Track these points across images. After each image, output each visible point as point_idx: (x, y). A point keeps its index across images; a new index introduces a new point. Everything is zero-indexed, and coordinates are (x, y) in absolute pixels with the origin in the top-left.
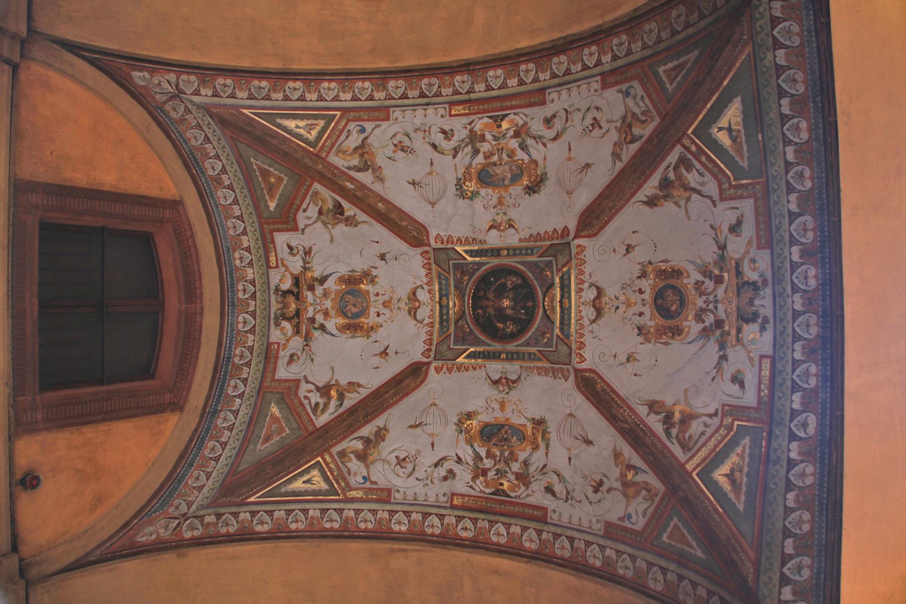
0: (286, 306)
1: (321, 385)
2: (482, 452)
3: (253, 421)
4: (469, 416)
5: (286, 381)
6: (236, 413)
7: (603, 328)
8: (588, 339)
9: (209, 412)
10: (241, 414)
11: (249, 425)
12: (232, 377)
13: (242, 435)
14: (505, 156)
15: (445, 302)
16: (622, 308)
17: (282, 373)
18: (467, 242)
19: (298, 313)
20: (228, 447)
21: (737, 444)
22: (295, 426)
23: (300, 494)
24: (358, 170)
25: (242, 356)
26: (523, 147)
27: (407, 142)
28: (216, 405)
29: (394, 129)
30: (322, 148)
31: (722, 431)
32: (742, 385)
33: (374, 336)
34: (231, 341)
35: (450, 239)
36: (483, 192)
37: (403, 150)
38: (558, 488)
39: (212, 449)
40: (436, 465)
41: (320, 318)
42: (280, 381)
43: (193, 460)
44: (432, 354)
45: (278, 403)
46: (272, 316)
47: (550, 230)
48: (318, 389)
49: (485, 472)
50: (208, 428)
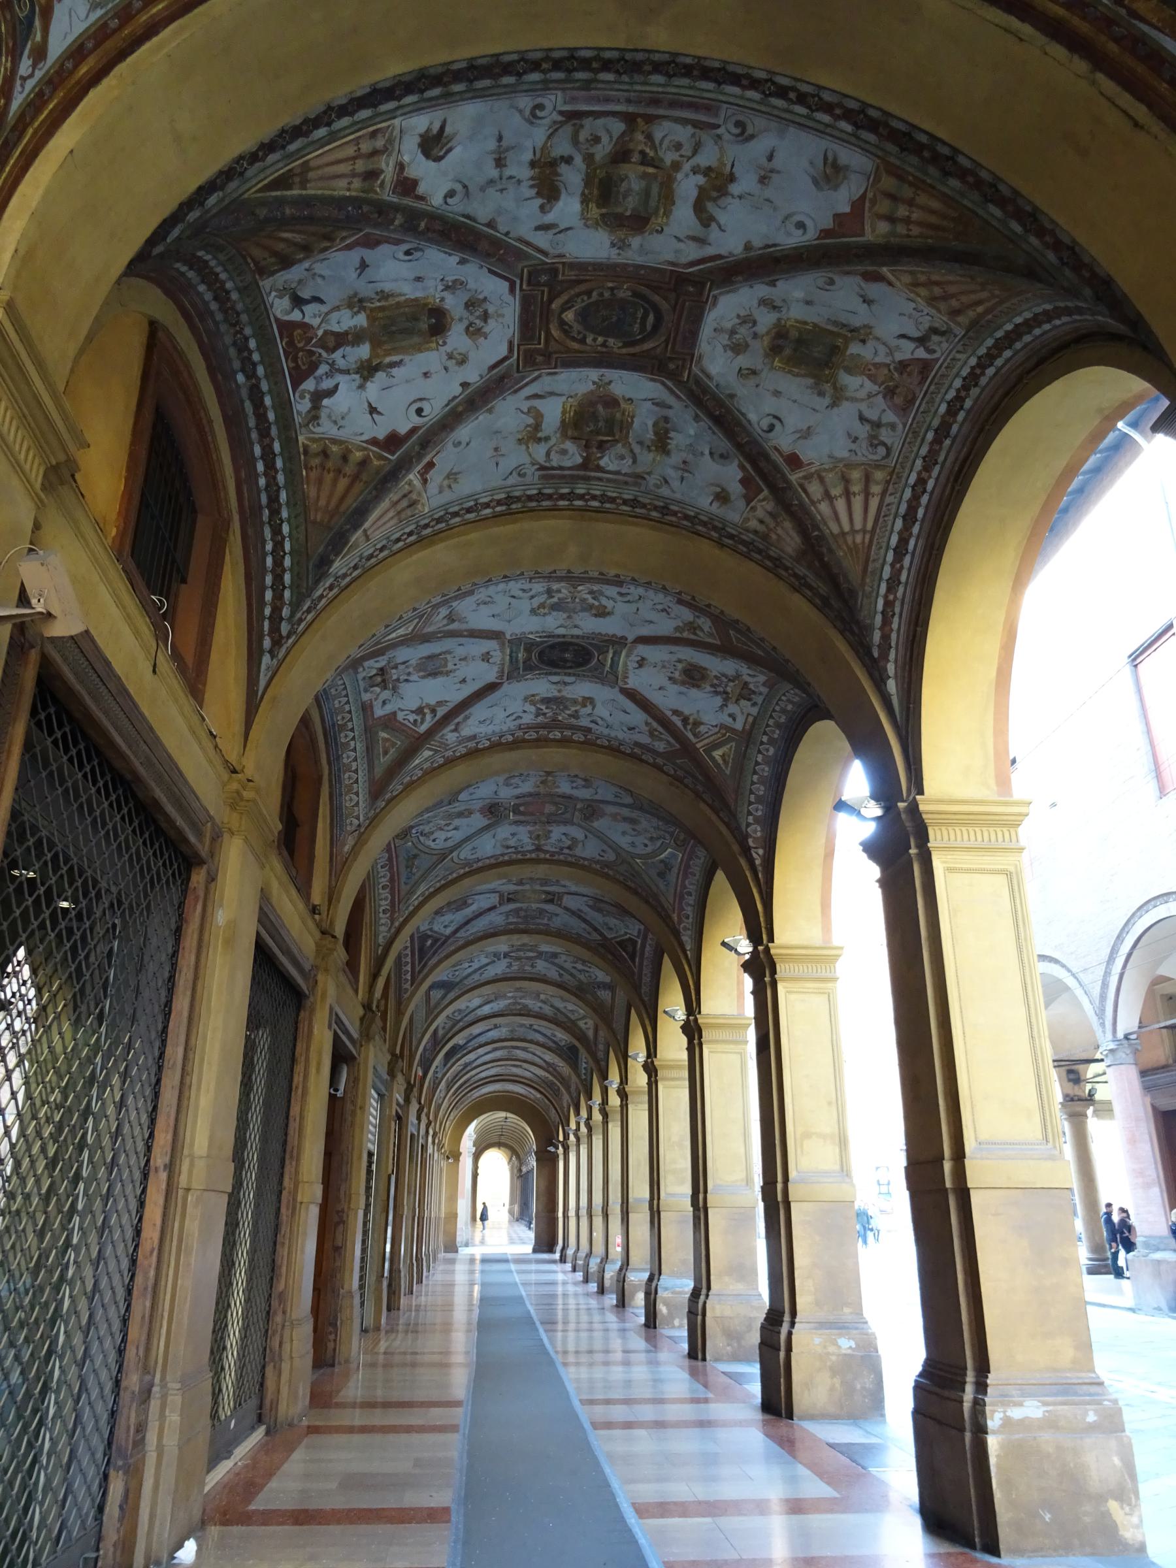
2: (543, 707)
3: (370, 750)
6: (354, 750)
7: (643, 672)
8: (631, 675)
12: (340, 732)
17: (379, 712)
19: (384, 681)
26: (594, 598)
32: (734, 719)
33: (452, 675)
36: (555, 613)
38: (600, 722)
39: (349, 778)
41: (402, 678)
42: (380, 718)
47: (611, 633)
48: (412, 712)
49: (544, 714)
50: (339, 769)
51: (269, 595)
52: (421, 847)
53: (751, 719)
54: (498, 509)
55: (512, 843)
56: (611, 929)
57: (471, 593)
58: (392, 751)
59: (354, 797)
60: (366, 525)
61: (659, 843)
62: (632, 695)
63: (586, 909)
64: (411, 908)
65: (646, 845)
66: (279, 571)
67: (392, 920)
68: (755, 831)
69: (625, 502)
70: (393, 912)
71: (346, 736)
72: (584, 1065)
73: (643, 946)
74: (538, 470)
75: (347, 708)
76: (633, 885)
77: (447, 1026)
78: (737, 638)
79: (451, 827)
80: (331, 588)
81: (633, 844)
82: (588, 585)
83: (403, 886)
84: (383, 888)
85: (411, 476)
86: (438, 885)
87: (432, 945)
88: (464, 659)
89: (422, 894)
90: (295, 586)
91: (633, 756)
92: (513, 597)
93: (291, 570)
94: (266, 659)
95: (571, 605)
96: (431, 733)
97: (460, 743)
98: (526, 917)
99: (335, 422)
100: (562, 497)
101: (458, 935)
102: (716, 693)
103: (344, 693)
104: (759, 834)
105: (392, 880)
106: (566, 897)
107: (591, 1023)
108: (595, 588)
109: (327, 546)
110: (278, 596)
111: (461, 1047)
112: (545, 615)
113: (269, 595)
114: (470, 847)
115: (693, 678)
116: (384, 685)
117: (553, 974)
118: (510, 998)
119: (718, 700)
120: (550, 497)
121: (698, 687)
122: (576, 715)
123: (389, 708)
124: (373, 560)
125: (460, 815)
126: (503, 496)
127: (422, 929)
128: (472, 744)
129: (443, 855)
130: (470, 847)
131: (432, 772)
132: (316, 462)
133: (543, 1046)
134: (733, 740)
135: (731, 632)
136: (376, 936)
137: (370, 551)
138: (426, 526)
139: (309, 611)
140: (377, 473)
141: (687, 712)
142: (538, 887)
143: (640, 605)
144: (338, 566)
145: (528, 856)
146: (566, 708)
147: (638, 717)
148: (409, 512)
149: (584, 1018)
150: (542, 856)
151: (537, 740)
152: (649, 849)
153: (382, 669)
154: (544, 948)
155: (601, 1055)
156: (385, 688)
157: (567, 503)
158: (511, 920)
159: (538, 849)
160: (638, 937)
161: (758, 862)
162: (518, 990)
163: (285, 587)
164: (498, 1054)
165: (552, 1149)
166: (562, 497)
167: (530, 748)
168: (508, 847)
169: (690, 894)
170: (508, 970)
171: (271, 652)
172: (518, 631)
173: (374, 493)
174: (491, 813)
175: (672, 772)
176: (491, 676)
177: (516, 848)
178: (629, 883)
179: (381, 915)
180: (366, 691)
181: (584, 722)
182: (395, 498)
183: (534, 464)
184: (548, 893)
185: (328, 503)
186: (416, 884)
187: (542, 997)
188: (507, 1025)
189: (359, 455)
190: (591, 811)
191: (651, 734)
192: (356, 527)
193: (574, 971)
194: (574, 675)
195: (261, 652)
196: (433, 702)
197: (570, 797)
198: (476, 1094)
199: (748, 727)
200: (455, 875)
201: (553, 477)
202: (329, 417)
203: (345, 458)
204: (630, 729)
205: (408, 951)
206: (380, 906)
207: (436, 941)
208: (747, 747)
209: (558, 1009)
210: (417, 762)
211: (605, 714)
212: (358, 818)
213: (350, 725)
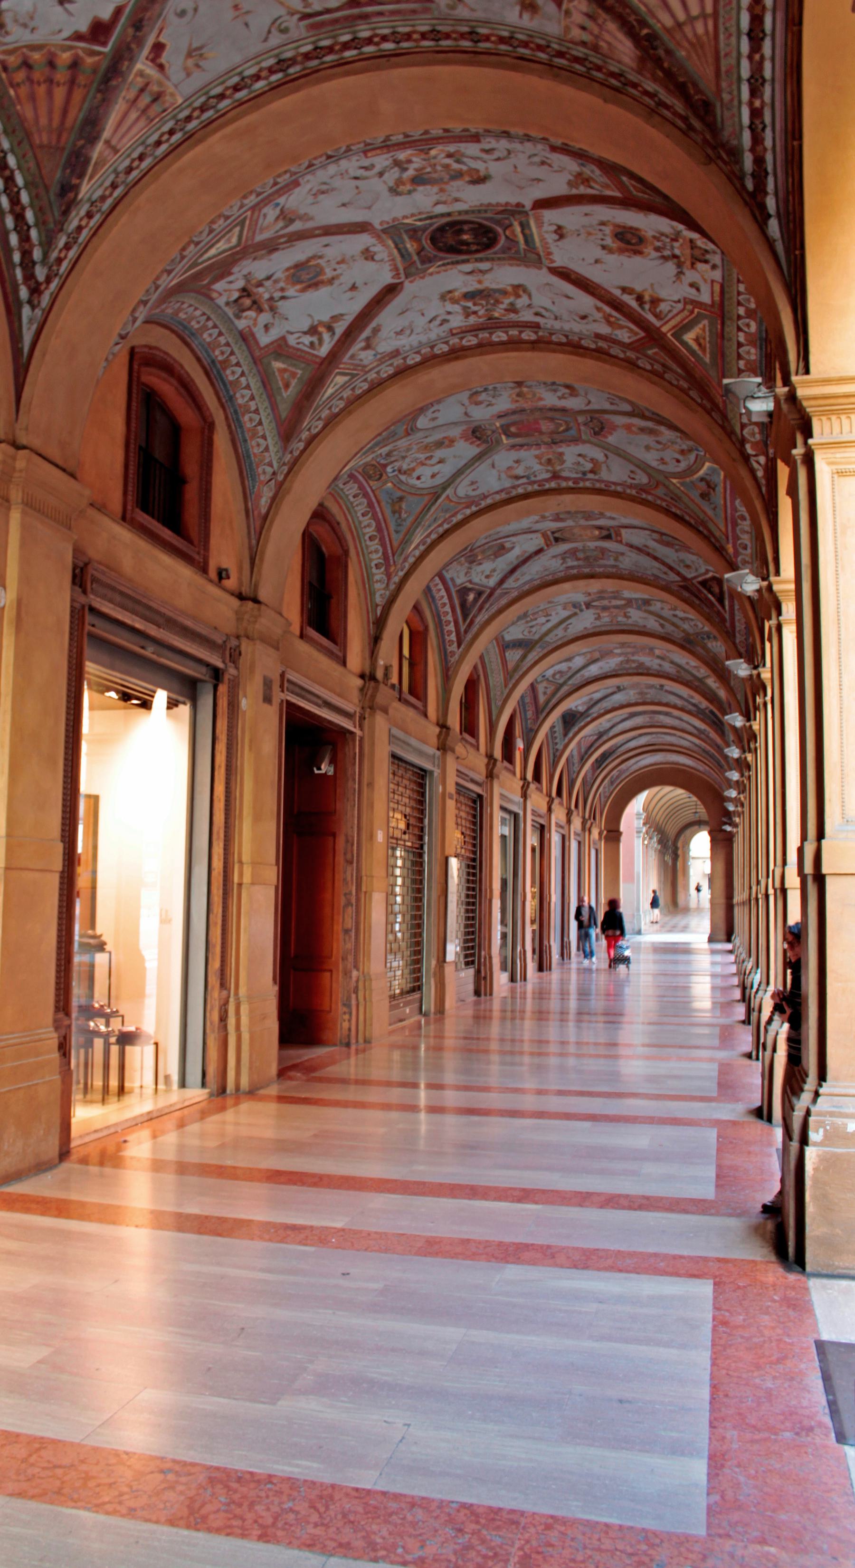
0: (242, 305)
1: (306, 329)
4: (450, 292)
5: (272, 343)
6: (248, 387)
8: (553, 249)
9: (226, 401)
10: (252, 385)
11: (265, 386)
12: (225, 369)
13: (264, 396)
14: (439, 168)
15: (401, 246)
16: (583, 236)
17: (264, 339)
18: (413, 215)
20: (261, 411)
21: (699, 322)
22: (303, 365)
23: (332, 394)
24: (286, 227)
25: (222, 353)
26: (458, 161)
27: (324, 187)
28: (227, 391)
29: (308, 187)
30: (247, 240)
31: (686, 313)
32: (698, 290)
33: (337, 282)
34: (207, 351)
35: (394, 220)
36: (421, 188)
37: (323, 192)
39: (251, 420)
40: (430, 321)
41: (277, 295)
42: (267, 346)
43: (243, 436)
44: (403, 276)
45: (276, 360)
46: (231, 316)
48: (305, 333)
49: (475, 313)
50: (236, 412)
51: (14, 239)
53: (717, 288)
54: (274, 78)
55: (520, 471)
56: (688, 567)
57: (296, 184)
58: (294, 382)
59: (261, 441)
60: (106, 135)
61: (692, 457)
62: (564, 274)
63: (652, 544)
64: (411, 560)
65: (678, 461)
66: (18, 209)
67: (389, 576)
68: (753, 434)
69: (424, 36)
71: (233, 373)
74: (301, 19)
75: (222, 340)
76: (678, 512)
77: (549, 691)
78: (634, 186)
80: (89, 215)
81: (662, 460)
82: (440, 147)
83: (394, 536)
85: (139, 66)
86: (441, 530)
87: (476, 600)
88: (342, 262)
89: (423, 542)
90: (40, 223)
91: (598, 350)
92: (356, 178)
93: (32, 205)
94: (26, 311)
95: (435, 176)
96: (334, 356)
97: (381, 361)
98: (586, 559)
99: (25, 26)
100: (346, 46)
101: (505, 586)
102: (665, 258)
103: (210, 324)
104: (758, 437)
105: (379, 529)
106: (623, 531)
108: (452, 148)
109: (64, 169)
110: (25, 238)
111: (583, 715)
112: (409, 192)
113: (14, 239)
114: (466, 482)
115: (628, 243)
116: (256, 306)
117: (652, 624)
118: (620, 655)
119: (670, 268)
120: (330, 50)
121: (640, 253)
122: (512, 309)
123: (275, 334)
124: (135, 174)
125: (439, 444)
126: (271, 62)
127: (458, 581)
128: (398, 362)
129: (435, 494)
131: (355, 402)
132: (20, 76)
133: (682, 709)
134: (705, 317)
135: (624, 179)
136: (372, 594)
137: (127, 163)
138: (189, 119)
139: (67, 247)
140: (95, 72)
141: (638, 288)
142: (582, 522)
143: (513, 160)
144: (86, 189)
145: (547, 486)
146: (498, 302)
147: (585, 302)
148: (156, 108)
149: (708, 677)
150: (564, 484)
151: (480, 345)
152: (683, 465)
153: (244, 290)
154: (627, 594)
156: (260, 310)
157: (354, 52)
158: (570, 563)
159: (555, 476)
161: (760, 474)
162: (623, 645)
163: (29, 227)
166: (346, 46)
167: (473, 356)
168: (517, 478)
169: (743, 518)
170: (598, 623)
171: (30, 302)
172: (387, 218)
173: (99, 96)
174: (479, 439)
175: (649, 367)
176: (386, 278)
177: (528, 477)
178: (674, 510)
179: (374, 570)
180: (238, 317)
181: (527, 316)
182: (132, 95)
183: (292, 14)
184: (600, 528)
185: (50, 120)
186: (410, 532)
187: (657, 652)
188: (633, 686)
189: (65, 57)
190: (598, 425)
191: (609, 323)
192: (93, 140)
193: (675, 620)
194: (487, 259)
195: (20, 305)
196: (326, 318)
197: (564, 410)
199: (717, 298)
200: (460, 517)
201: (322, 24)
202: (16, 21)
203: (51, 64)
204: (584, 317)
205: (448, 608)
206: (371, 560)
207: (479, 594)
208: (723, 324)
210: (330, 391)
211: (548, 304)
212: (270, 465)
213: (233, 360)
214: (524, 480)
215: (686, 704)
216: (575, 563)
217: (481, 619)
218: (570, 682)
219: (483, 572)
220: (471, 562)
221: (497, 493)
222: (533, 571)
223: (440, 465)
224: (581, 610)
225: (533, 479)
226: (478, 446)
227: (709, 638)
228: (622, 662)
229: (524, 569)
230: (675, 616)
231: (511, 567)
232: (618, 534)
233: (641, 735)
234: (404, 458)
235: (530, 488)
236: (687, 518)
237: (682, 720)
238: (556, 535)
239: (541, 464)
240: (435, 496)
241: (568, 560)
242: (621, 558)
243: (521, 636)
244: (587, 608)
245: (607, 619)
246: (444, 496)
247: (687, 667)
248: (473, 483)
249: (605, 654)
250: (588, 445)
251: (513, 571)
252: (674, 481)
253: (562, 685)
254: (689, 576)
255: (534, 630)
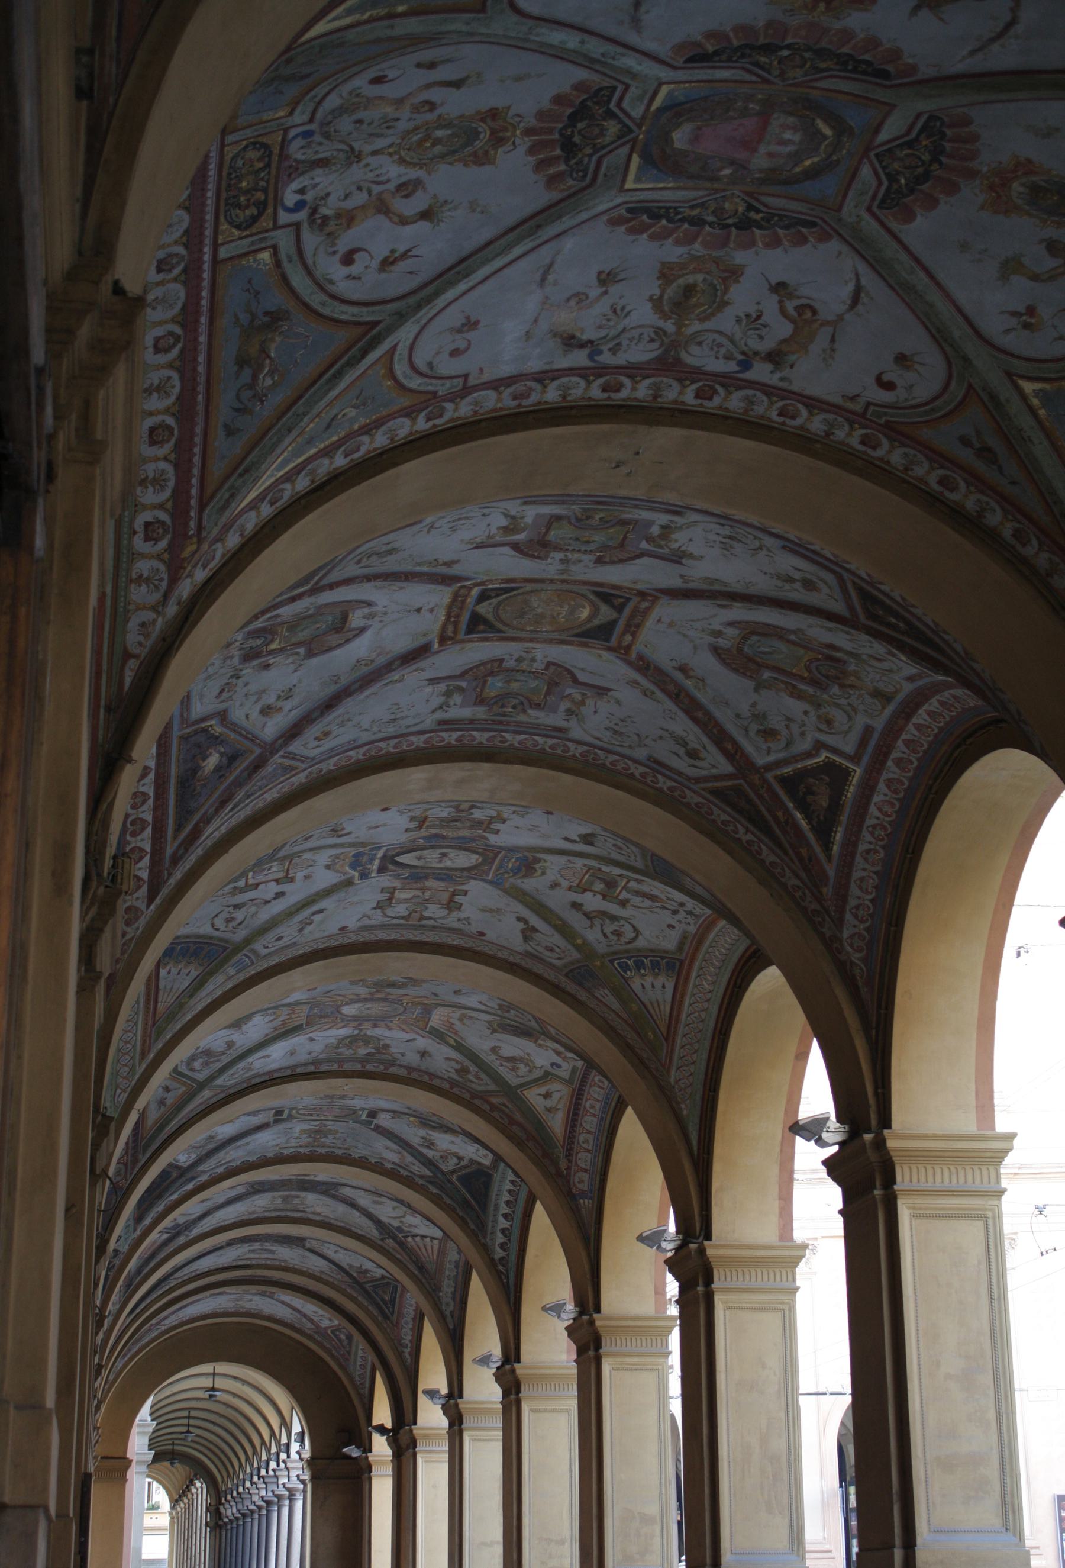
52: (298, 280)
55: (588, 323)
56: (769, 734)
64: (233, 540)
70: (180, 537)
72: (503, 1223)
73: (868, 788)
77: (171, 1099)
79: (419, 202)
84: (155, 436)
86: (325, 467)
98: (501, 699)
101: (296, 747)
105: (184, 409)
107: (560, 1092)
114: (453, 317)
118: (347, 1020)
127: (198, 709)
130: (453, 317)
133: (392, 1174)
150: (672, 392)
155: (582, 1181)
160: (855, 758)
164: (260, 1203)
165: (353, 1451)
168: (570, 342)
170: (378, 918)
174: (569, 148)
179: (138, 542)
184: (606, 595)
186: (261, 444)
187: (437, 1018)
193: (575, 920)
198: (173, 1317)
200: (381, 440)
206: (139, 507)
207: (233, 758)
209: (474, 1057)
214: (579, 358)
215: (409, 1159)
216: (467, 713)
217: (215, 830)
218: (219, 1082)
219: (261, 692)
220: (249, 656)
221: (496, 385)
222: (365, 720)
223: (423, 226)
224: (364, 875)
225: (606, 358)
226: (552, 181)
227: (639, 965)
228: (341, 1041)
229: (349, 705)
230: (576, 906)
231: (333, 688)
232: (633, 627)
233: (230, 1243)
234: (354, 156)
235: (578, 390)
236: (994, 518)
237: (353, 1205)
238: (484, 609)
239: (657, 303)
240: (368, 335)
241: (457, 699)
242: (587, 710)
243: (206, 929)
244: (381, 870)
245: (401, 909)
246: (386, 346)
247: (490, 1059)
248: (470, 324)
249: (321, 1012)
250: (835, 245)
251: (330, 704)
252: (1028, 387)
253: (202, 1086)
254: (761, 761)
255: (239, 915)
